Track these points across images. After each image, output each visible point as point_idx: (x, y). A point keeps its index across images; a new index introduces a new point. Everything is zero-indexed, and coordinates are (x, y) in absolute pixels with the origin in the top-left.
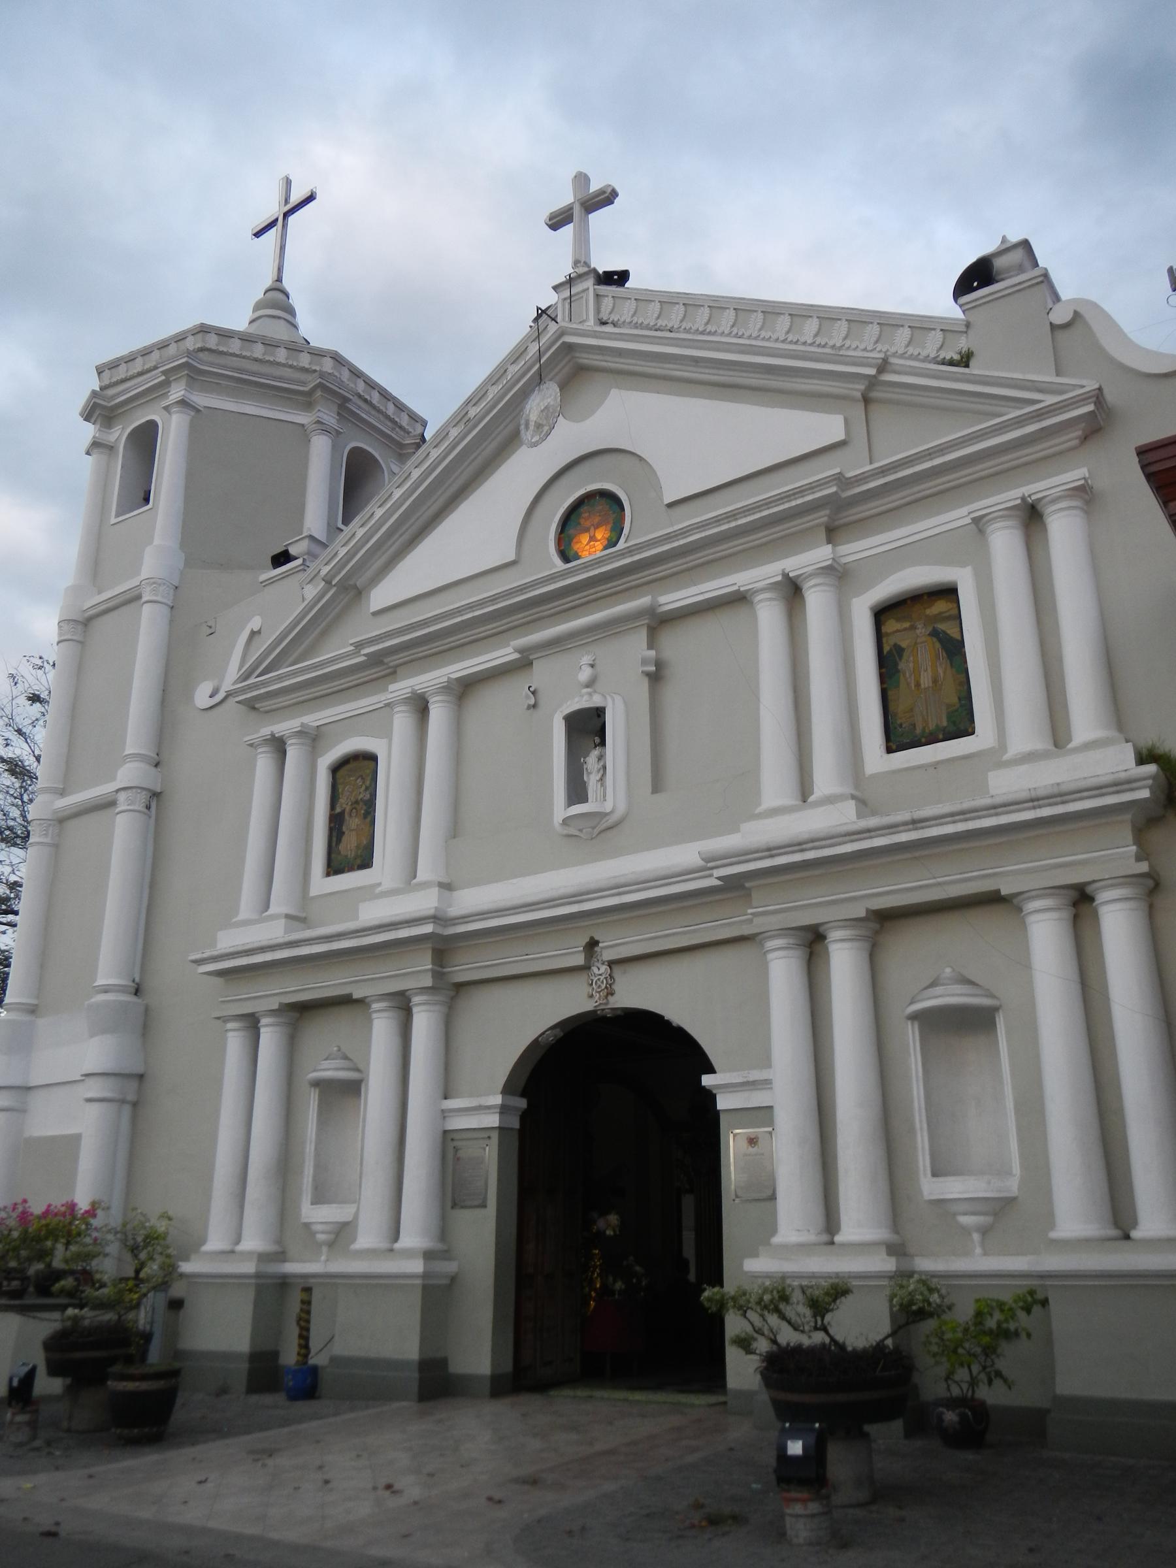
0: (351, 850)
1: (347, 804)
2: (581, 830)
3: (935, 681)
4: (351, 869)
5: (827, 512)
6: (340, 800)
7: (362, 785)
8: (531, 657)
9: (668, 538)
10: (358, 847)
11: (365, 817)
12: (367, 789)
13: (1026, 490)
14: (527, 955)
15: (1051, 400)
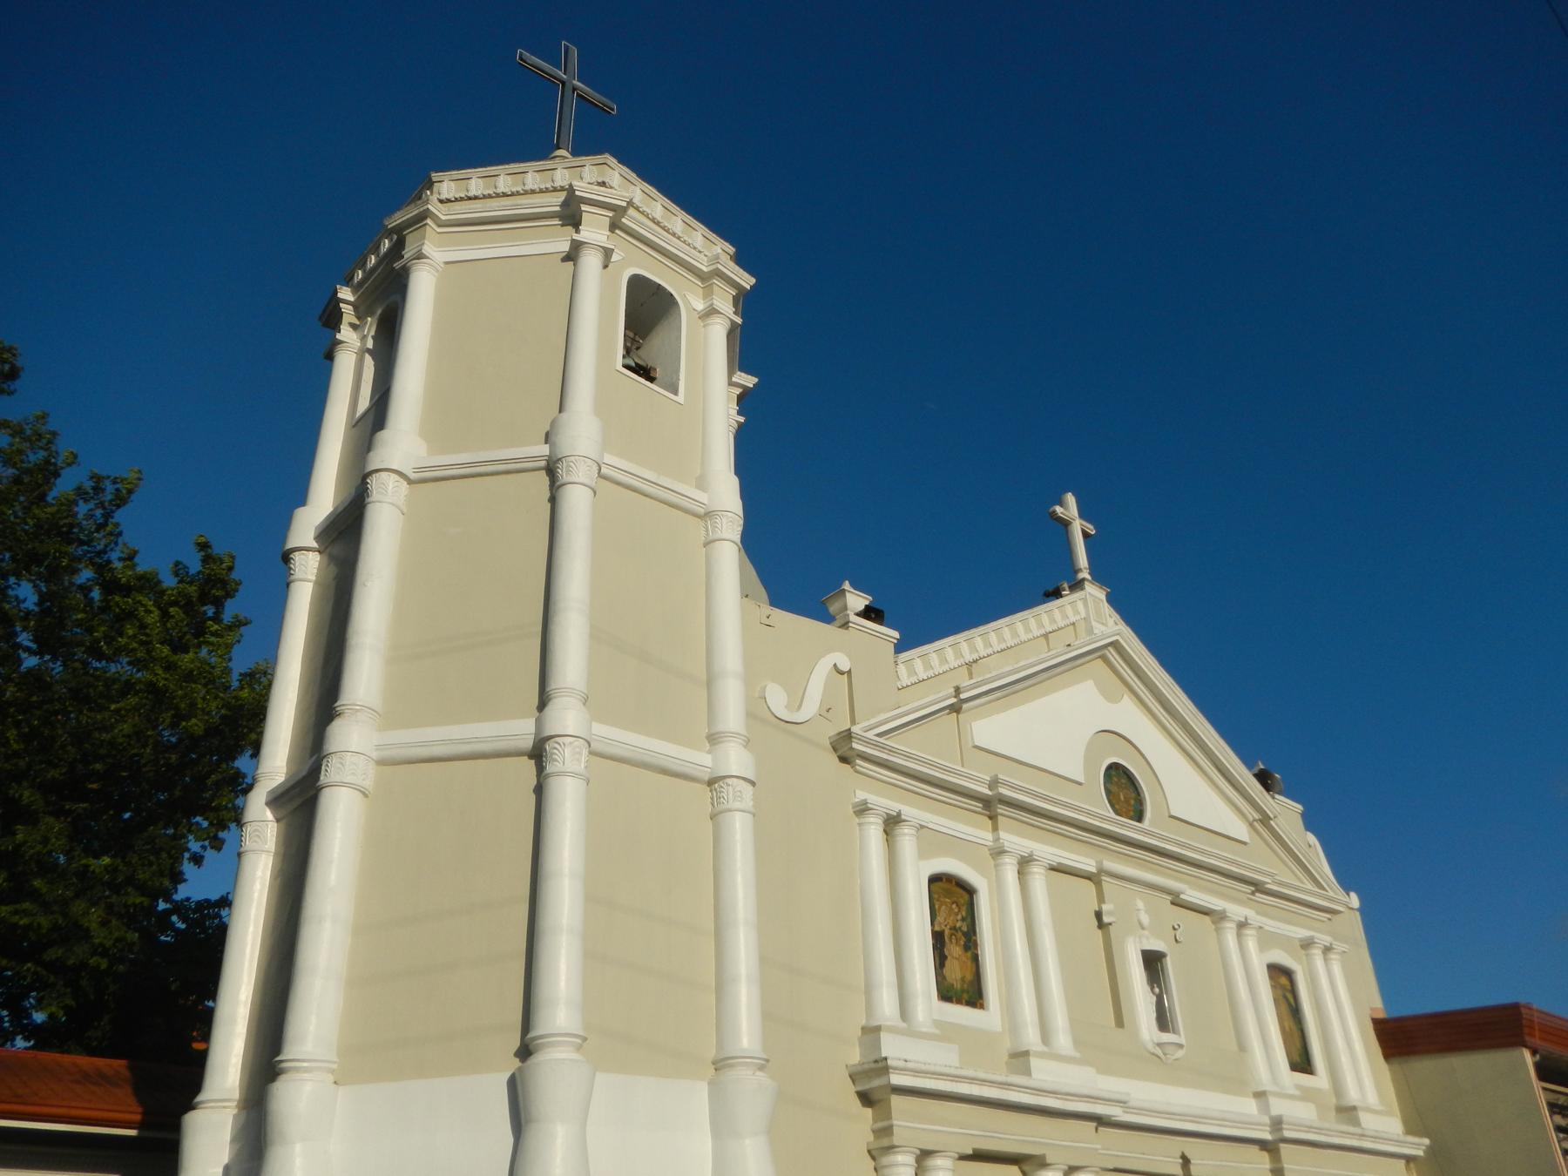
0: (957, 981)
1: (946, 926)
2: (1165, 1054)
3: (1291, 1029)
4: (959, 1002)
5: (1253, 889)
6: (938, 918)
7: (957, 915)
8: (1103, 878)
9: (1202, 852)
10: (963, 979)
11: (967, 948)
12: (963, 919)
13: (1316, 935)
14: (1144, 1154)
15: (1331, 893)
